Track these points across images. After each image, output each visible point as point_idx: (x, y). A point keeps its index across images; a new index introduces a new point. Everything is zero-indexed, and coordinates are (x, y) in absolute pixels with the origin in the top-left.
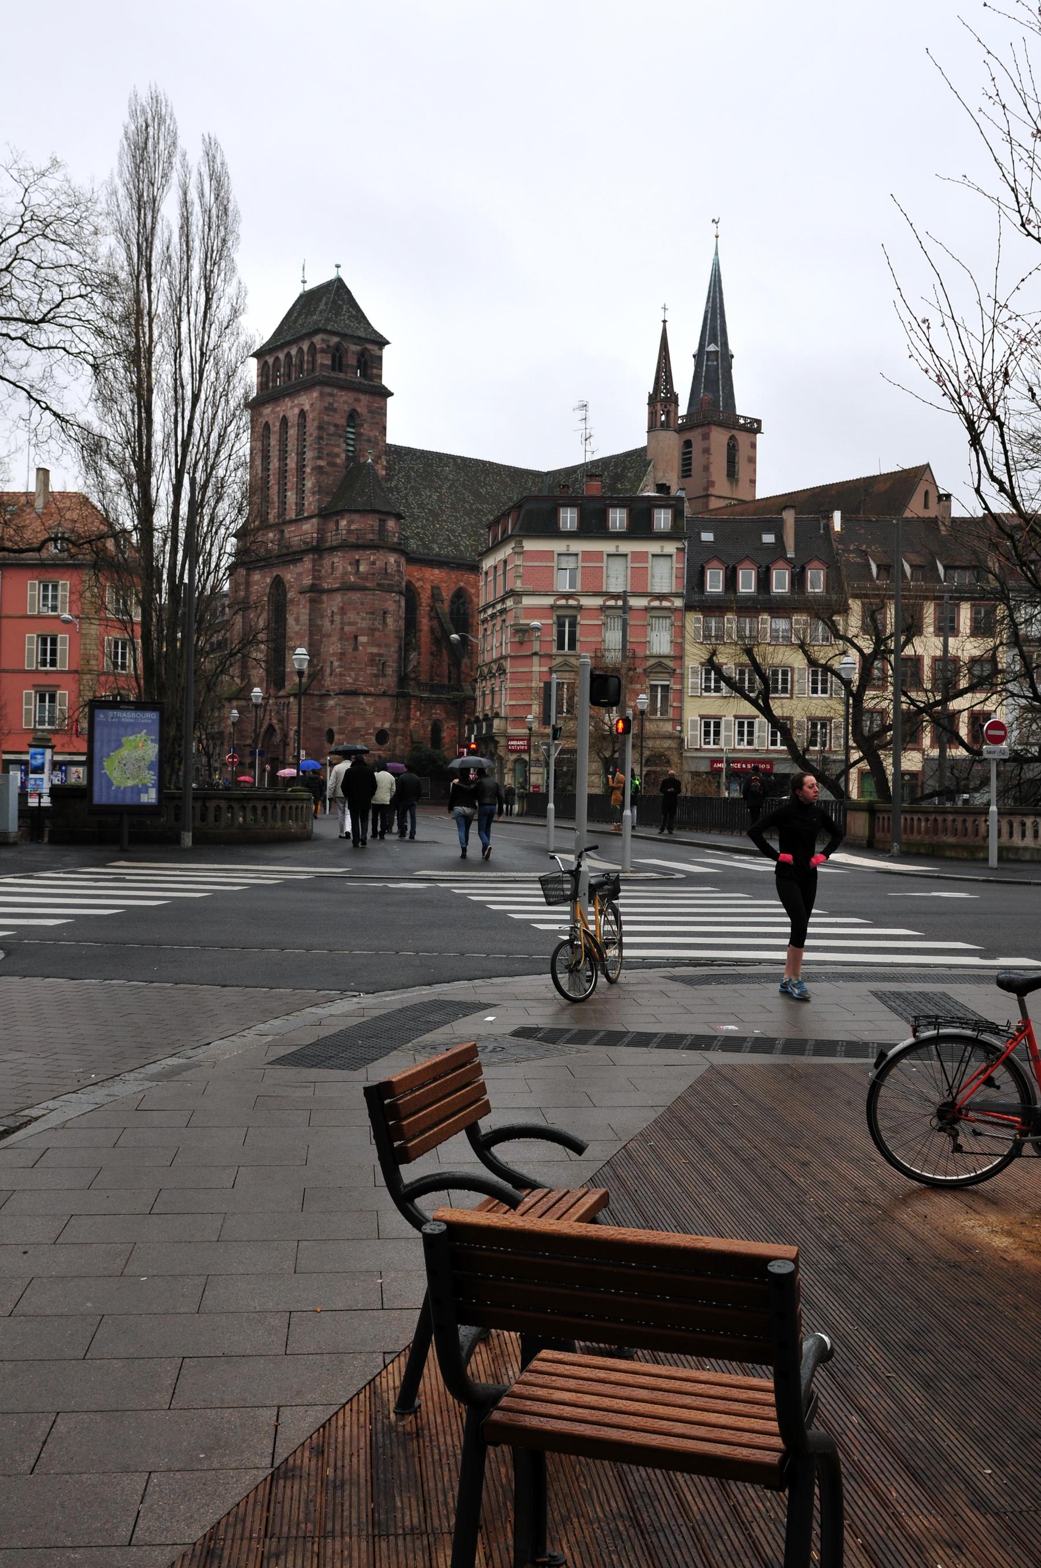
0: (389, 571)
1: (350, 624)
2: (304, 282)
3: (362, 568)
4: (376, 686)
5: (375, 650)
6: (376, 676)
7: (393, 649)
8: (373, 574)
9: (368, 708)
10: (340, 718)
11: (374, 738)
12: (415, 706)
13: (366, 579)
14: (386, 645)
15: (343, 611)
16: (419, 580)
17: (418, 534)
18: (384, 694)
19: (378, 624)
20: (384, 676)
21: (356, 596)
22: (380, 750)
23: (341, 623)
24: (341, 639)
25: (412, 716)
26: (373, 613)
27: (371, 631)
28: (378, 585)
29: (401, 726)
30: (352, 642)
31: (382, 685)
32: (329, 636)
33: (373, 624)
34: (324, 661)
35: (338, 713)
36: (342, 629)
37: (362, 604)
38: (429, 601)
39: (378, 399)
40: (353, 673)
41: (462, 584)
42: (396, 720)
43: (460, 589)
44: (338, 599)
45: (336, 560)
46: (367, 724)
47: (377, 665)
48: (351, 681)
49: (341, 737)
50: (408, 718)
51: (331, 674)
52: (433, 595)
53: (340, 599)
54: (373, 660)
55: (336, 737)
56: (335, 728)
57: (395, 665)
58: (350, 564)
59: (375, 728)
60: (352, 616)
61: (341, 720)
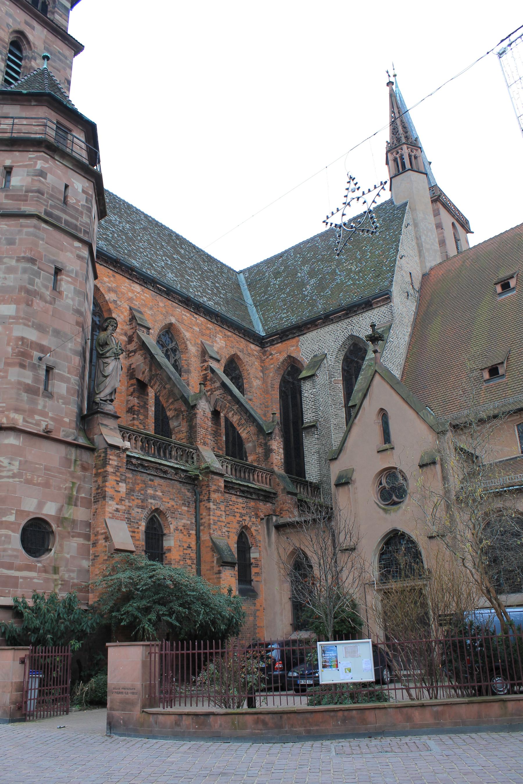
0: (71, 200)
3: (16, 181)
5: (32, 335)
6: (30, 390)
7: (70, 345)
8: (40, 192)
12: (118, 467)
13: (24, 199)
14: (57, 333)
16: (110, 290)
17: (106, 239)
18: (46, 436)
19: (42, 283)
20: (48, 394)
22: (29, 568)
25: (109, 491)
26: (32, 261)
28: (46, 213)
29: (80, 514)
31: (44, 414)
33: (31, 282)
37: (11, 242)
38: (127, 327)
39: (60, 43)
41: (173, 320)
42: (71, 500)
43: (171, 324)
47: (34, 368)
52: (133, 318)
57: (74, 379)
59: (20, 513)
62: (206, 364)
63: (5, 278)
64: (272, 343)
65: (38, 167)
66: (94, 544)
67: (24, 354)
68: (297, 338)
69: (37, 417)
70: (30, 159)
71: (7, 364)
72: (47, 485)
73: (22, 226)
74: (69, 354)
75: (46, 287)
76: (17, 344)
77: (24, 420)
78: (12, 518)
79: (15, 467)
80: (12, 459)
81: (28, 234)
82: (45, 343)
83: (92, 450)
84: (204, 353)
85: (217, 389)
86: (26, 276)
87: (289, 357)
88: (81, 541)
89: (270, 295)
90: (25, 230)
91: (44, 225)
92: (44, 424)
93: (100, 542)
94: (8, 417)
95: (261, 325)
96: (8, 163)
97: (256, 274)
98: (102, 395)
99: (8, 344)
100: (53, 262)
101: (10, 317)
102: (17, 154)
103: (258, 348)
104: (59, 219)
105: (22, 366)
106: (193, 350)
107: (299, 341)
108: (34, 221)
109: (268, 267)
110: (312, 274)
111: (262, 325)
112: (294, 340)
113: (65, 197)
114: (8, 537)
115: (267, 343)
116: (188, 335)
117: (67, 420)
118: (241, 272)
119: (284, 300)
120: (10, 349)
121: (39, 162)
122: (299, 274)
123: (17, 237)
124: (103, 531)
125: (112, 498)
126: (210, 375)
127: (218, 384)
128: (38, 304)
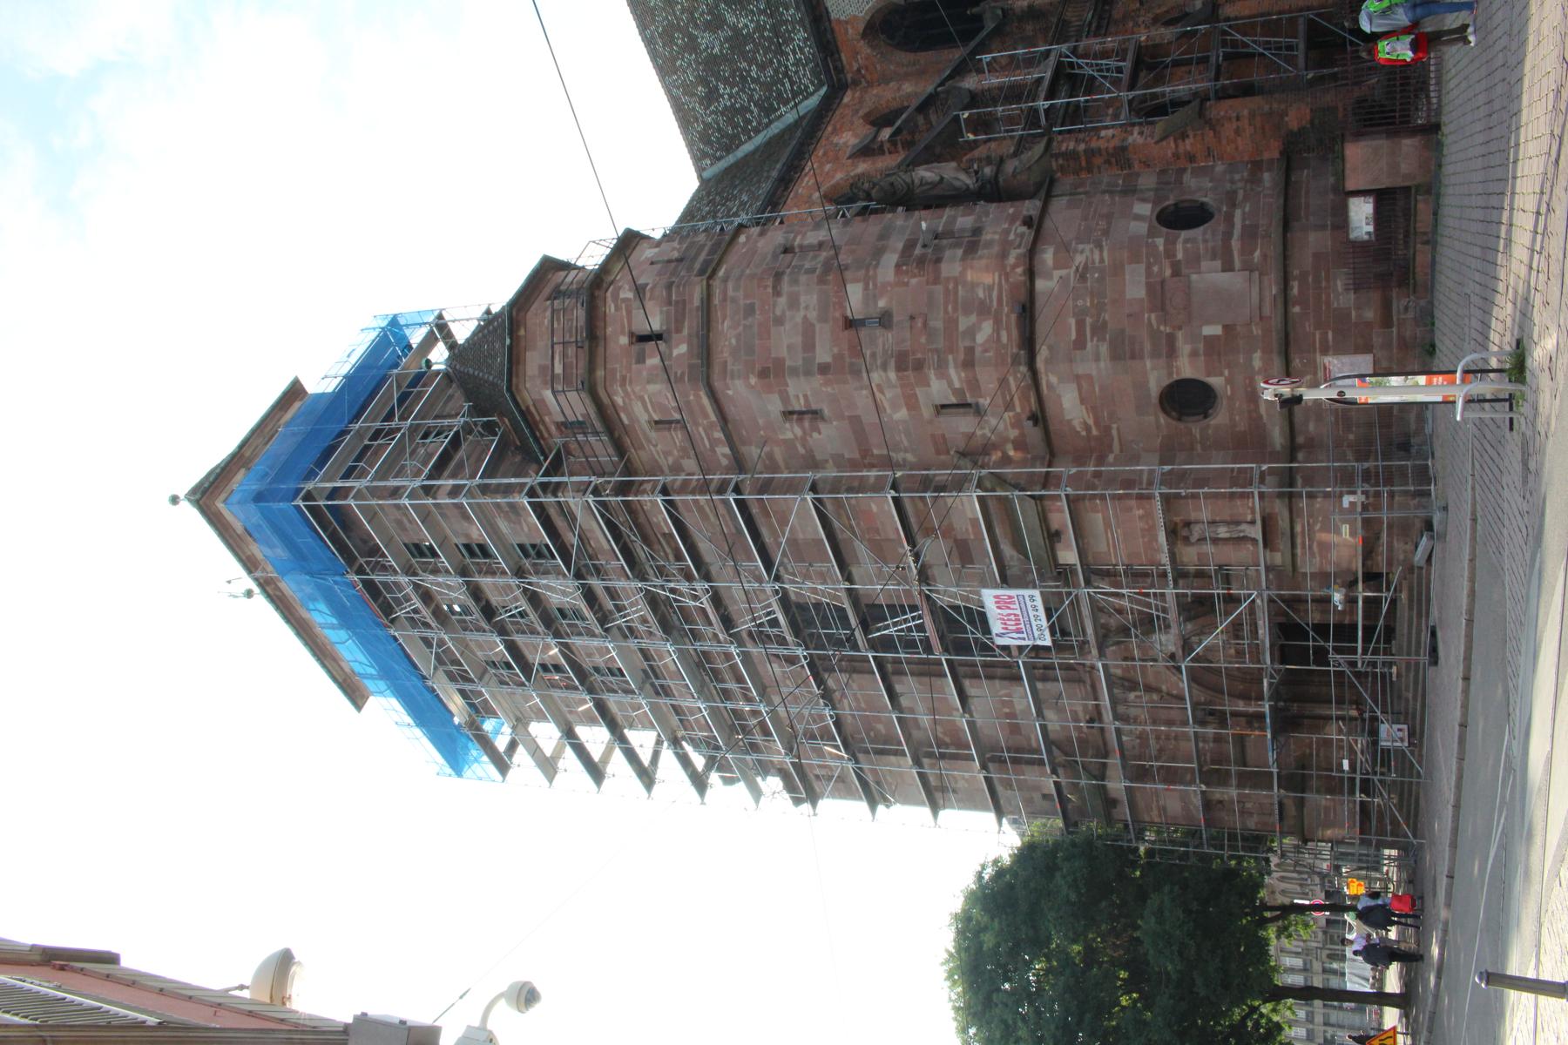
0: (676, 255)
1: (809, 346)
4: (1005, 248)
5: (891, 259)
7: (899, 222)
8: (669, 286)
9: (1079, 259)
10: (1116, 356)
11: (1184, 234)
13: (681, 306)
15: (771, 373)
18: (1035, 224)
21: (727, 333)
22: (1229, 219)
23: (808, 373)
24: (856, 373)
25: (1115, 142)
26: (778, 276)
27: (834, 272)
28: (701, 272)
29: (1147, 181)
30: (863, 333)
32: (855, 421)
34: (941, 444)
35: (1096, 364)
36: (824, 369)
37: (750, 310)
40: (964, 322)
42: (1130, 191)
44: (740, 391)
45: (643, 418)
46: (1135, 258)
47: (939, 250)
48: (987, 328)
49: (1184, 348)
50: (1120, 157)
51: (978, 411)
53: (739, 384)
54: (921, 261)
55: (1187, 369)
56: (1156, 381)
58: (641, 359)
59: (1151, 233)
60: (785, 342)
61: (1124, 351)
62: (886, 146)
63: (807, 308)
64: (840, 70)
65: (630, 295)
66: (1191, 158)
67: (921, 261)
68: (833, 24)
69: (1012, 237)
70: (617, 308)
71: (936, 281)
72: (1109, 217)
73: (725, 300)
74: (911, 222)
75: (815, 257)
76: (907, 272)
77: (1019, 247)
78: (1160, 242)
79: (1088, 247)
80: (1076, 251)
81: (736, 289)
82: (900, 245)
83: (1052, 182)
84: (867, 151)
85: (927, 118)
86: (803, 278)
87: (864, 35)
88: (1187, 177)
89: (751, 98)
90: (730, 293)
91: (721, 273)
92: (1024, 229)
93: (1188, 148)
94: (1014, 267)
95: (806, 103)
96: (624, 340)
97: (708, 143)
98: (968, 181)
99: (907, 284)
100: (775, 256)
101: (866, 288)
102: (609, 330)
103: (849, 93)
104: (707, 263)
105: (938, 260)
106: (863, 167)
107: (838, 21)
108: (717, 284)
109: (697, 120)
110: (716, 24)
111: (806, 98)
112: (836, 28)
113: (669, 261)
114: (1186, 241)
115: (839, 80)
116: (839, 176)
117: (1011, 211)
118: (700, 177)
119: (762, 67)
120: (914, 281)
121: (622, 295)
122: (716, 50)
123: (742, 302)
124: (1172, 145)
125: (1124, 140)
126: (905, 135)
127: (921, 120)
128: (844, 258)
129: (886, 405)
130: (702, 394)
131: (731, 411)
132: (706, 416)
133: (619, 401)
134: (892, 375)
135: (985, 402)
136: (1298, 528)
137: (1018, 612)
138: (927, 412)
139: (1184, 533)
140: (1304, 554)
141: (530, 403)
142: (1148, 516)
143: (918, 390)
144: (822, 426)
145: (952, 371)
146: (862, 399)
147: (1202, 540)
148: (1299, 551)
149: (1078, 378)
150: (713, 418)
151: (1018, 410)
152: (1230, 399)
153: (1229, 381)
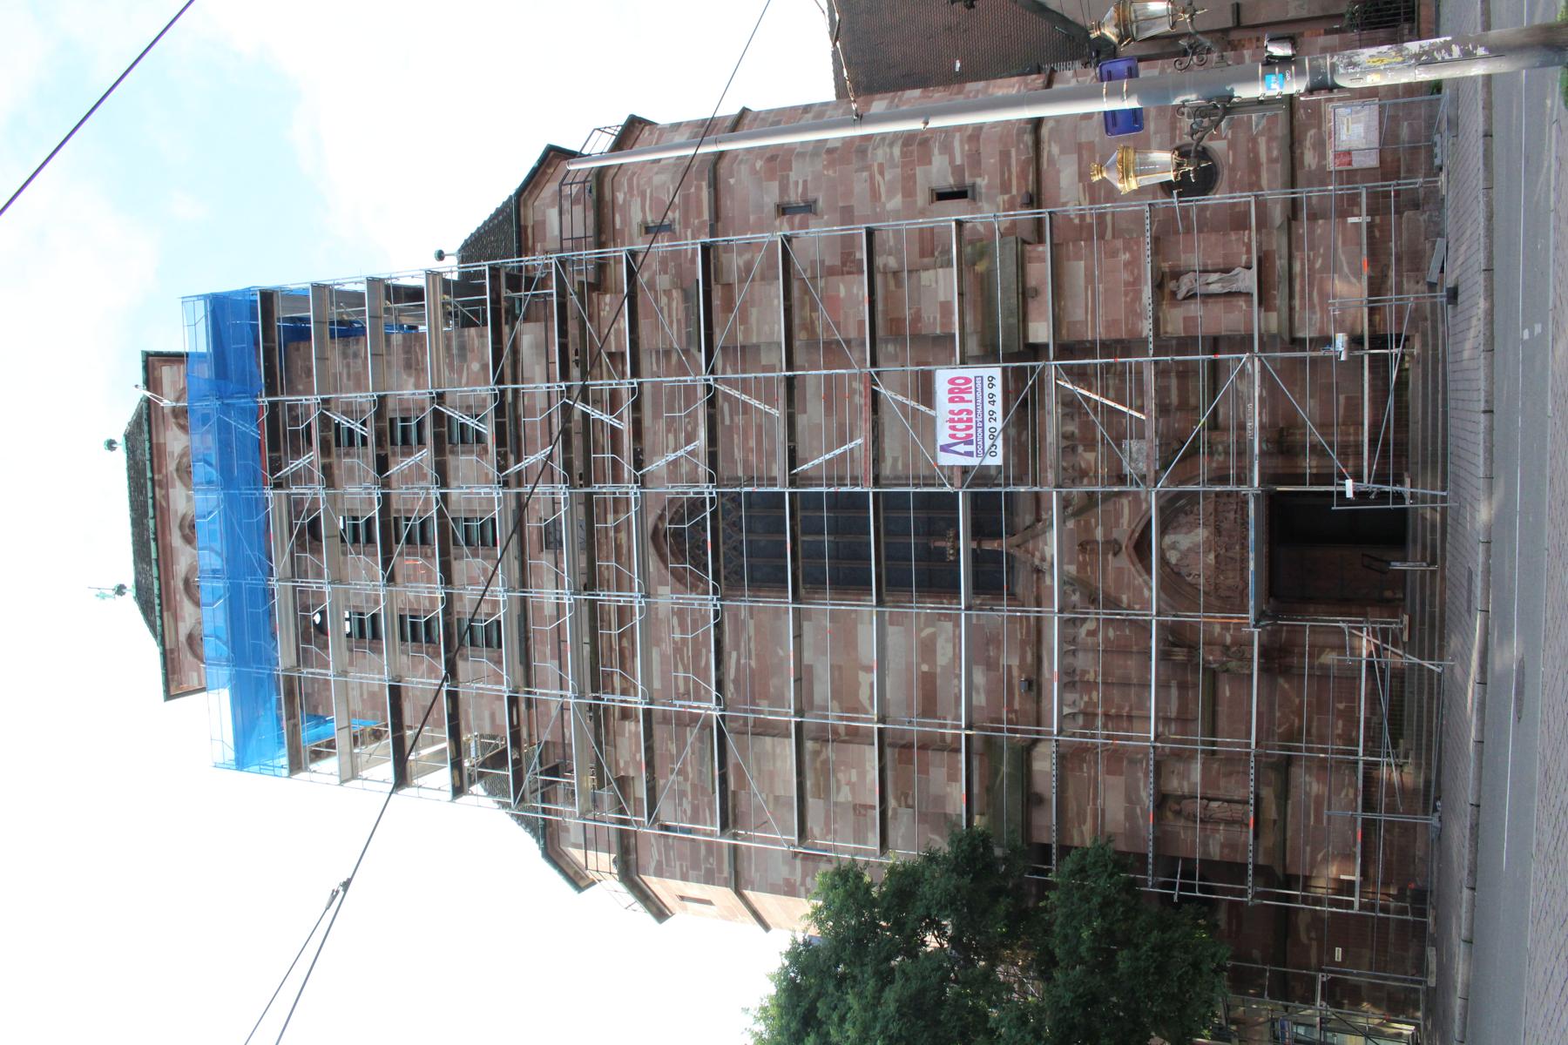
2: (120, 590)
45: (636, 217)
129: (883, 190)
130: (704, 184)
131: (727, 203)
132: (700, 214)
133: (620, 197)
134: (897, 151)
135: (982, 182)
136: (1297, 268)
137: (971, 407)
138: (922, 198)
139: (1172, 285)
140: (1303, 307)
141: (530, 223)
142: (1133, 263)
143: (919, 170)
144: (812, 220)
145: (957, 144)
146: (860, 185)
147: (1191, 296)
148: (1297, 303)
149: (1079, 148)
150: (706, 216)
151: (1014, 192)
152: (1233, 169)
153: (1232, 145)
